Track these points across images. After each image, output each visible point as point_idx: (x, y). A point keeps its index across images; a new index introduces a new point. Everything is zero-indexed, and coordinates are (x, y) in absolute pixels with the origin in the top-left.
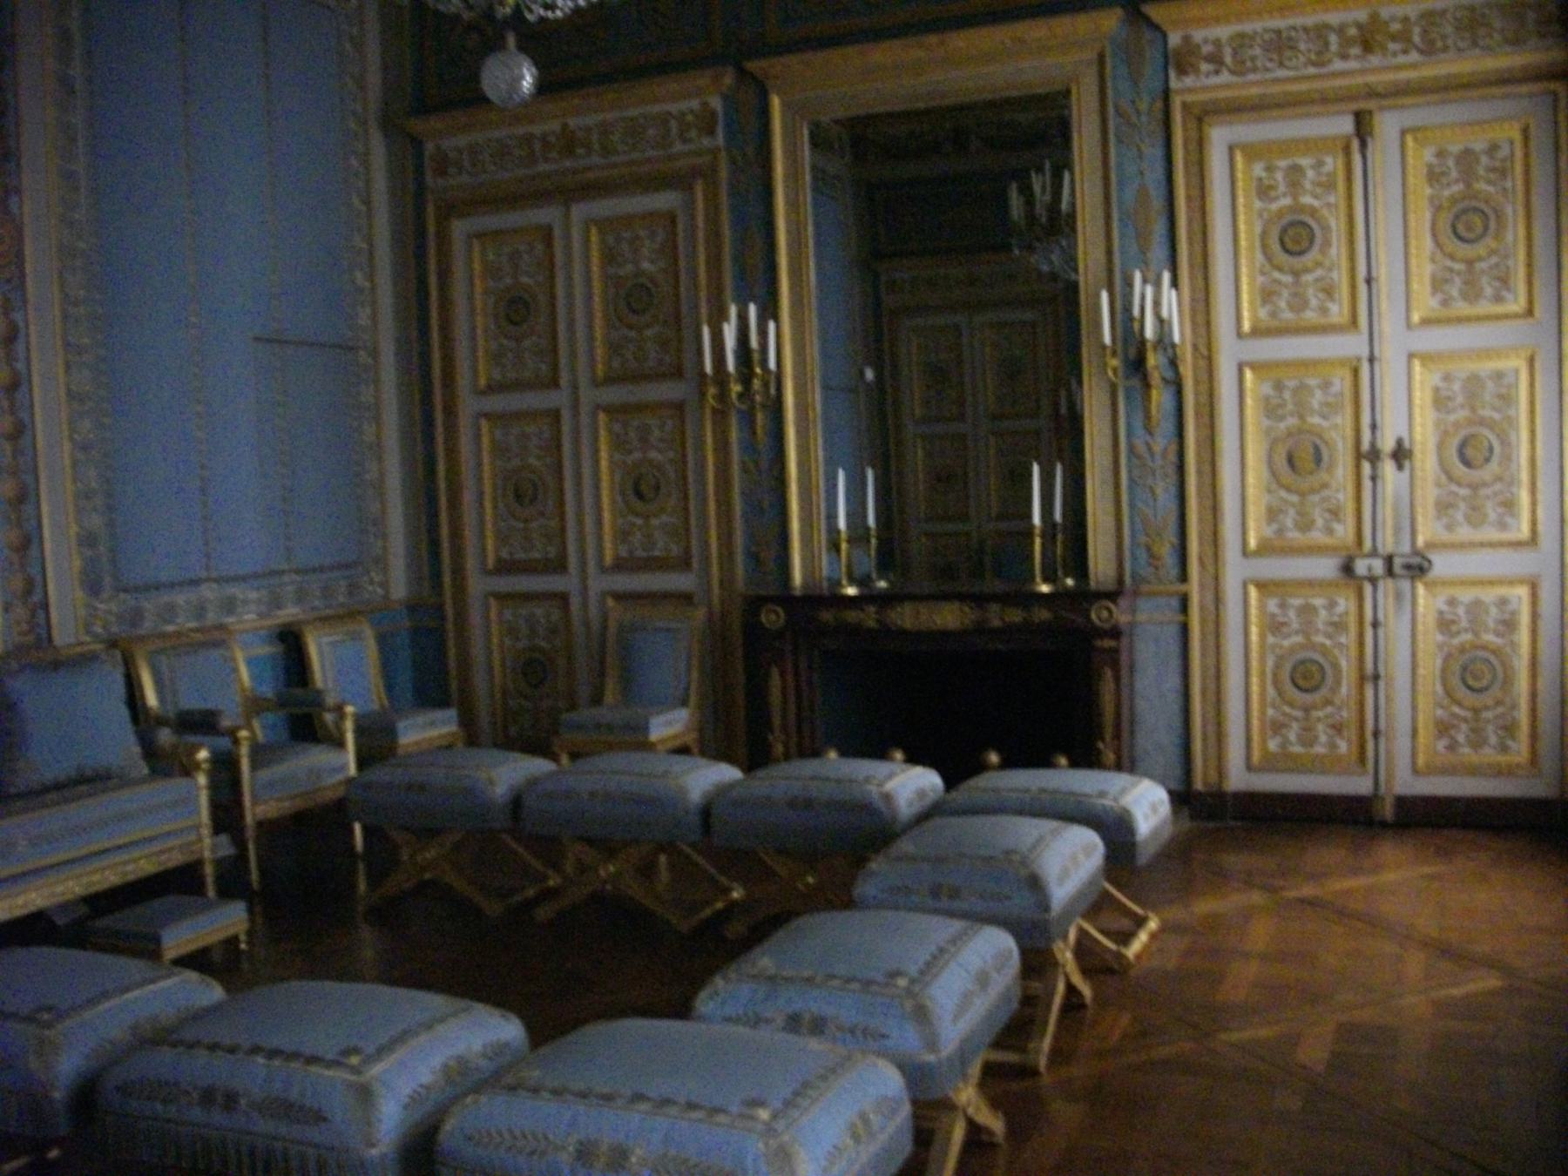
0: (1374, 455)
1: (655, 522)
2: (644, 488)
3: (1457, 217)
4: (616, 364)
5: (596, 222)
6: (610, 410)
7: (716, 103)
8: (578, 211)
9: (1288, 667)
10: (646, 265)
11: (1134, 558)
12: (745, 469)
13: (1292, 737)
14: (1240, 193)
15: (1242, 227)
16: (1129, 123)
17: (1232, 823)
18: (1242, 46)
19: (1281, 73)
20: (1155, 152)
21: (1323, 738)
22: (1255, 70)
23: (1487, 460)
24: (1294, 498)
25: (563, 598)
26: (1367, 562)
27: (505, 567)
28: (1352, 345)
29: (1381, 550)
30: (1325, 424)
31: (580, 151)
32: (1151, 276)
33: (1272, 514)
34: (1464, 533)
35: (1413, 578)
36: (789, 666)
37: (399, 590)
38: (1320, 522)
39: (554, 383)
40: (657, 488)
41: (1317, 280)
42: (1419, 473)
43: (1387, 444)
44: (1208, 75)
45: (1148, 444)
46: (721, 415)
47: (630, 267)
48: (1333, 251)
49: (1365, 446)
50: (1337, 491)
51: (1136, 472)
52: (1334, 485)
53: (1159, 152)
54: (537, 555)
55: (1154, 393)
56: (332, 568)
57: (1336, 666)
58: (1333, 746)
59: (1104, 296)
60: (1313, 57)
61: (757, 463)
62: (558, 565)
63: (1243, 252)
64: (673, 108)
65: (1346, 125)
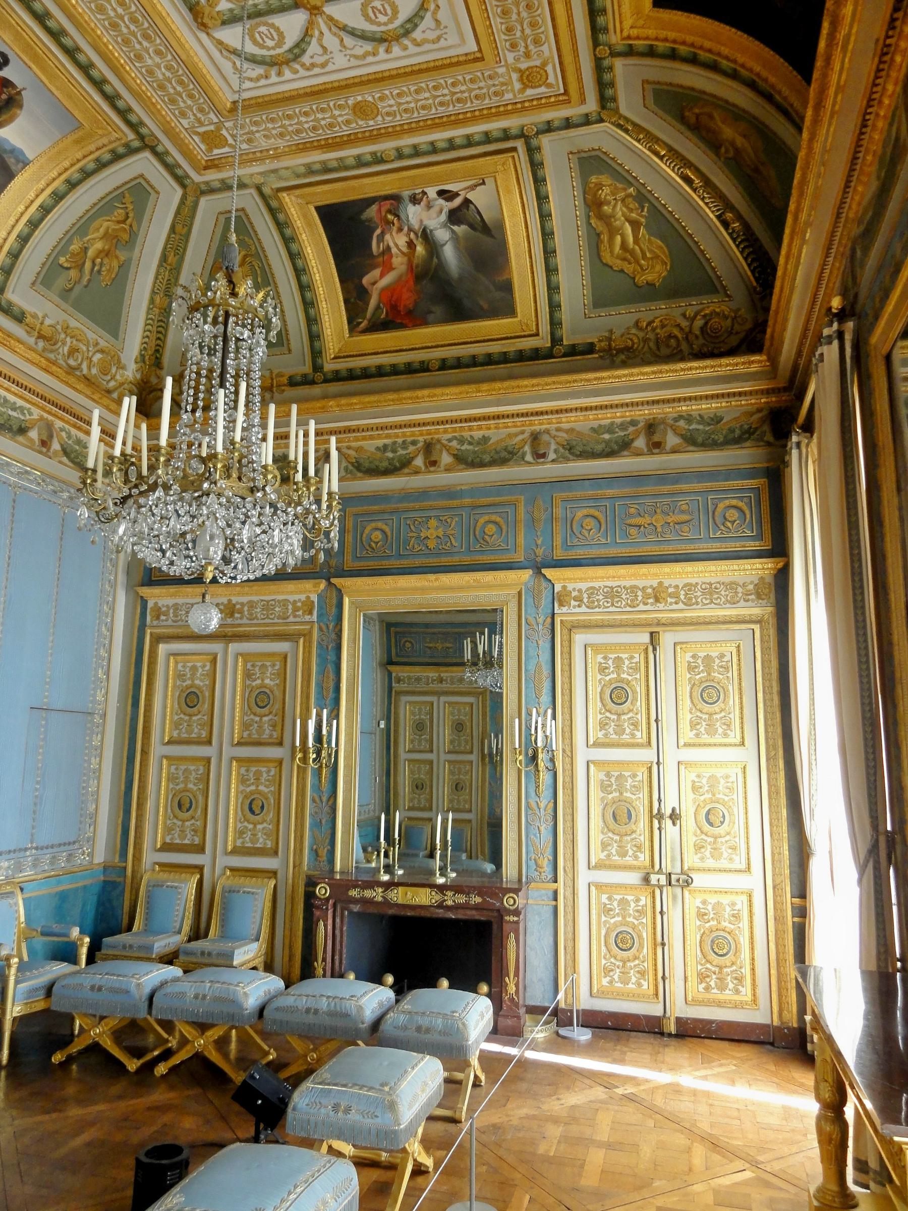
1: (260, 827)
2: (254, 807)
4: (245, 734)
5: (241, 654)
6: (239, 760)
7: (314, 598)
8: (233, 647)
10: (267, 681)
12: (313, 800)
13: (616, 977)
14: (589, 670)
15: (590, 688)
18: (592, 593)
19: (611, 609)
20: (545, 645)
21: (634, 980)
23: (722, 823)
24: (617, 838)
25: (200, 869)
27: (167, 847)
28: (649, 755)
29: (664, 871)
30: (634, 797)
31: (237, 615)
32: (541, 711)
33: (604, 846)
34: (710, 863)
36: (330, 922)
37: (100, 858)
38: (630, 853)
39: (209, 742)
40: (262, 807)
41: (629, 719)
43: (668, 812)
44: (574, 607)
46: (302, 771)
47: (259, 682)
49: (655, 811)
52: (638, 832)
53: (548, 645)
54: (186, 842)
56: (60, 845)
57: (640, 937)
59: (517, 720)
61: (320, 797)
62: (200, 849)
64: (292, 598)
65: (646, 638)
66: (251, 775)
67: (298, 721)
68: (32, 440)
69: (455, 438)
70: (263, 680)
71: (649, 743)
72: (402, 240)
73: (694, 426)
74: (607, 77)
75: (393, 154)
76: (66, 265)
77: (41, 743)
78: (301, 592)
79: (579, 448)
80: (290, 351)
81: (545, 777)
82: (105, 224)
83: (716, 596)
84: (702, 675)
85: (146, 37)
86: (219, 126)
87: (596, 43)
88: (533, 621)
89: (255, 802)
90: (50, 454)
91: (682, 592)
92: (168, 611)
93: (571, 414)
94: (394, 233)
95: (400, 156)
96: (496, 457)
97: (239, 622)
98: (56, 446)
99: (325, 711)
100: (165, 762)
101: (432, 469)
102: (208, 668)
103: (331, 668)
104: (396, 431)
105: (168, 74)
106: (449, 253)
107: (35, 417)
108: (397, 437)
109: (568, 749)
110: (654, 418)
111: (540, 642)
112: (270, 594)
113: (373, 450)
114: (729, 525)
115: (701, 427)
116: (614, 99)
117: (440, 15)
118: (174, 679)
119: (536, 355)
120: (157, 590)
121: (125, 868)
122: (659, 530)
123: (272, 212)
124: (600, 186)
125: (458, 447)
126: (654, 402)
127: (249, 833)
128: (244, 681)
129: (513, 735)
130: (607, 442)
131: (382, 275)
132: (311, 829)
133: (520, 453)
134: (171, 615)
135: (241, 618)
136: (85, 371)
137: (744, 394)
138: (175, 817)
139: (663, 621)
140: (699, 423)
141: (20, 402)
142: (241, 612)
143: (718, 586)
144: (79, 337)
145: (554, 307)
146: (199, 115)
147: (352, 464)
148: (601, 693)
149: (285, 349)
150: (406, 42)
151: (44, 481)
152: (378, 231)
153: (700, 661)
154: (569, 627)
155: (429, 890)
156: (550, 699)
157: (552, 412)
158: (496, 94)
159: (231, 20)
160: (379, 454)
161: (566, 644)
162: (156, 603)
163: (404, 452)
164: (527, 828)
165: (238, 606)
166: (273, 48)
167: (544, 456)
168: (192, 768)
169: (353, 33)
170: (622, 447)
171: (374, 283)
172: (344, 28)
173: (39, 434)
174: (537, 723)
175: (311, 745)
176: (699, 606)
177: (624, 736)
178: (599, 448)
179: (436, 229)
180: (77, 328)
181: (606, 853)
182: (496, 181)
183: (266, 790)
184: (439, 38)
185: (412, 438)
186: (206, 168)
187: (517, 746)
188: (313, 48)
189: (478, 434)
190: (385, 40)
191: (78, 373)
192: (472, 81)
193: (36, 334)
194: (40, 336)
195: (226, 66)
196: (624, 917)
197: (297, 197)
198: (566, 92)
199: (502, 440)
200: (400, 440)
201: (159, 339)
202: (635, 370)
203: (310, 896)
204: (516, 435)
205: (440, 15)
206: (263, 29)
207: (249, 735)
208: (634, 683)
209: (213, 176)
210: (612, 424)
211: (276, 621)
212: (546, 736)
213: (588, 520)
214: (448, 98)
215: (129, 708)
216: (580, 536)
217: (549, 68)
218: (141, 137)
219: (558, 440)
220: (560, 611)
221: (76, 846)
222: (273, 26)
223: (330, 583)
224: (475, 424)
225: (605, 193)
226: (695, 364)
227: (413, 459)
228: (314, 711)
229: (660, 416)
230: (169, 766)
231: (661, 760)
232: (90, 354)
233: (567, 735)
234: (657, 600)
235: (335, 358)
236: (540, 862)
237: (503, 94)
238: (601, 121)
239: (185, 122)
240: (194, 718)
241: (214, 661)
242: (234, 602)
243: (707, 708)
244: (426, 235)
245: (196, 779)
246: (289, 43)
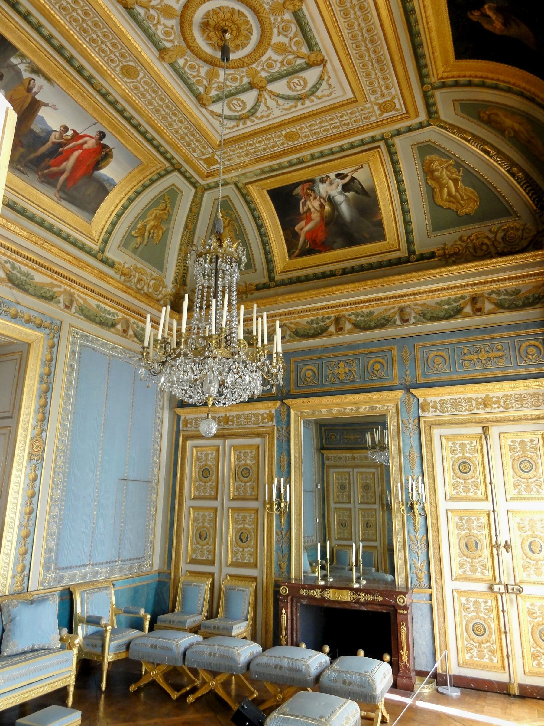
1: (246, 550)
2: (242, 537)
3: (521, 463)
5: (233, 446)
6: (233, 509)
7: (274, 411)
8: (229, 442)
10: (248, 462)
11: (411, 578)
12: (277, 534)
13: (475, 654)
14: (444, 451)
18: (443, 403)
20: (415, 436)
21: (487, 656)
22: (448, 411)
23: (541, 551)
25: (212, 575)
26: (499, 586)
28: (488, 505)
29: (503, 583)
30: (479, 533)
31: (230, 423)
32: (415, 478)
33: (461, 565)
34: (534, 578)
36: (289, 610)
37: (156, 567)
38: (479, 570)
39: (216, 498)
40: (247, 538)
41: (472, 482)
43: (503, 543)
44: (432, 412)
46: (270, 516)
47: (243, 462)
48: (478, 472)
49: (494, 543)
51: (411, 546)
53: (417, 436)
54: (204, 558)
55: (417, 518)
56: (134, 559)
57: (489, 627)
58: (491, 660)
62: (212, 563)
64: (261, 412)
65: (480, 431)
66: (240, 518)
67: (267, 485)
68: (119, 330)
69: (353, 313)
70: (246, 461)
71: (487, 498)
72: (316, 204)
73: (502, 297)
74: (431, 101)
75: (309, 157)
76: (135, 235)
77: (124, 499)
78: (266, 409)
79: (429, 315)
80: (256, 270)
81: (420, 520)
82: (155, 212)
83: (525, 402)
84: (519, 453)
85: (174, 114)
86: (213, 154)
87: (423, 84)
88: (406, 422)
89: (243, 535)
90: (128, 337)
91: (502, 401)
92: (192, 421)
93: (423, 295)
94: (312, 200)
95: (313, 157)
96: (378, 323)
97: (231, 427)
98: (131, 332)
99: (282, 479)
100: (191, 510)
101: (340, 332)
102: (214, 455)
103: (285, 453)
104: (318, 312)
105: (186, 131)
106: (345, 209)
107: (120, 317)
108: (319, 315)
109: (433, 502)
110: (476, 294)
111: (412, 435)
112: (248, 410)
113: (305, 323)
114: (530, 357)
115: (506, 297)
116: (436, 112)
117: (331, 82)
118: (196, 461)
119: (399, 262)
120: (185, 410)
121: (170, 574)
122: (484, 362)
123: (244, 196)
124: (432, 161)
125: (355, 319)
126: (475, 284)
127: (240, 553)
128: (235, 462)
129: (397, 493)
130: (447, 311)
131: (306, 224)
132: (276, 552)
133: (392, 320)
134: (194, 424)
135: (232, 425)
136: (146, 291)
137: (534, 275)
138: (198, 543)
139: (490, 419)
140: (505, 295)
141: (112, 310)
142: (232, 421)
143: (526, 396)
144: (143, 273)
145: (408, 233)
146: (202, 150)
147: (293, 332)
148: (452, 466)
149: (253, 270)
150: (313, 98)
151: (125, 352)
152: (303, 200)
153: (517, 444)
154: (429, 425)
155: (349, 592)
156: (420, 470)
157: (411, 295)
158: (366, 118)
159: (218, 99)
160: (309, 326)
161: (428, 435)
162: (185, 418)
163: (324, 324)
164: (409, 553)
165: (230, 418)
166: (241, 111)
167: (407, 321)
168: (207, 514)
169: (283, 97)
170: (457, 312)
171: (302, 229)
172: (278, 96)
173: (122, 327)
174: (412, 485)
175: (274, 500)
176: (514, 409)
177: (470, 494)
178: (442, 314)
179: (336, 196)
180: (141, 268)
181: (462, 570)
182: (369, 166)
183: (249, 527)
184: (331, 94)
185: (328, 315)
186: (207, 177)
188: (262, 107)
189: (366, 311)
190: (301, 99)
191: (142, 292)
192: (351, 113)
193: (120, 273)
194: (123, 274)
195: (216, 123)
196: (477, 613)
197: (257, 186)
198: (407, 112)
199: (381, 313)
200: (320, 317)
201: (184, 270)
202: (461, 266)
203: (277, 593)
204: (390, 309)
205: (331, 82)
206: (235, 102)
207: (239, 494)
208: (474, 459)
209: (211, 181)
210: (449, 299)
211: (252, 426)
212: (419, 494)
213: (437, 358)
214: (338, 124)
215: (172, 478)
216: (433, 368)
217: (396, 101)
218: (173, 165)
219: (416, 310)
220: (423, 415)
221: (143, 560)
222: (240, 100)
223: (283, 403)
224: (364, 304)
225: (435, 165)
226: (499, 260)
227: (328, 327)
228: (276, 479)
229: (479, 292)
230: (194, 513)
231: (495, 509)
232: (148, 281)
233: (432, 493)
234: (486, 406)
235: (281, 272)
236: (419, 575)
237: (370, 118)
238: (430, 125)
239: (195, 155)
240: (208, 484)
241: (218, 450)
242: (228, 415)
243: (524, 475)
244: (330, 200)
245: (209, 520)
246: (249, 107)
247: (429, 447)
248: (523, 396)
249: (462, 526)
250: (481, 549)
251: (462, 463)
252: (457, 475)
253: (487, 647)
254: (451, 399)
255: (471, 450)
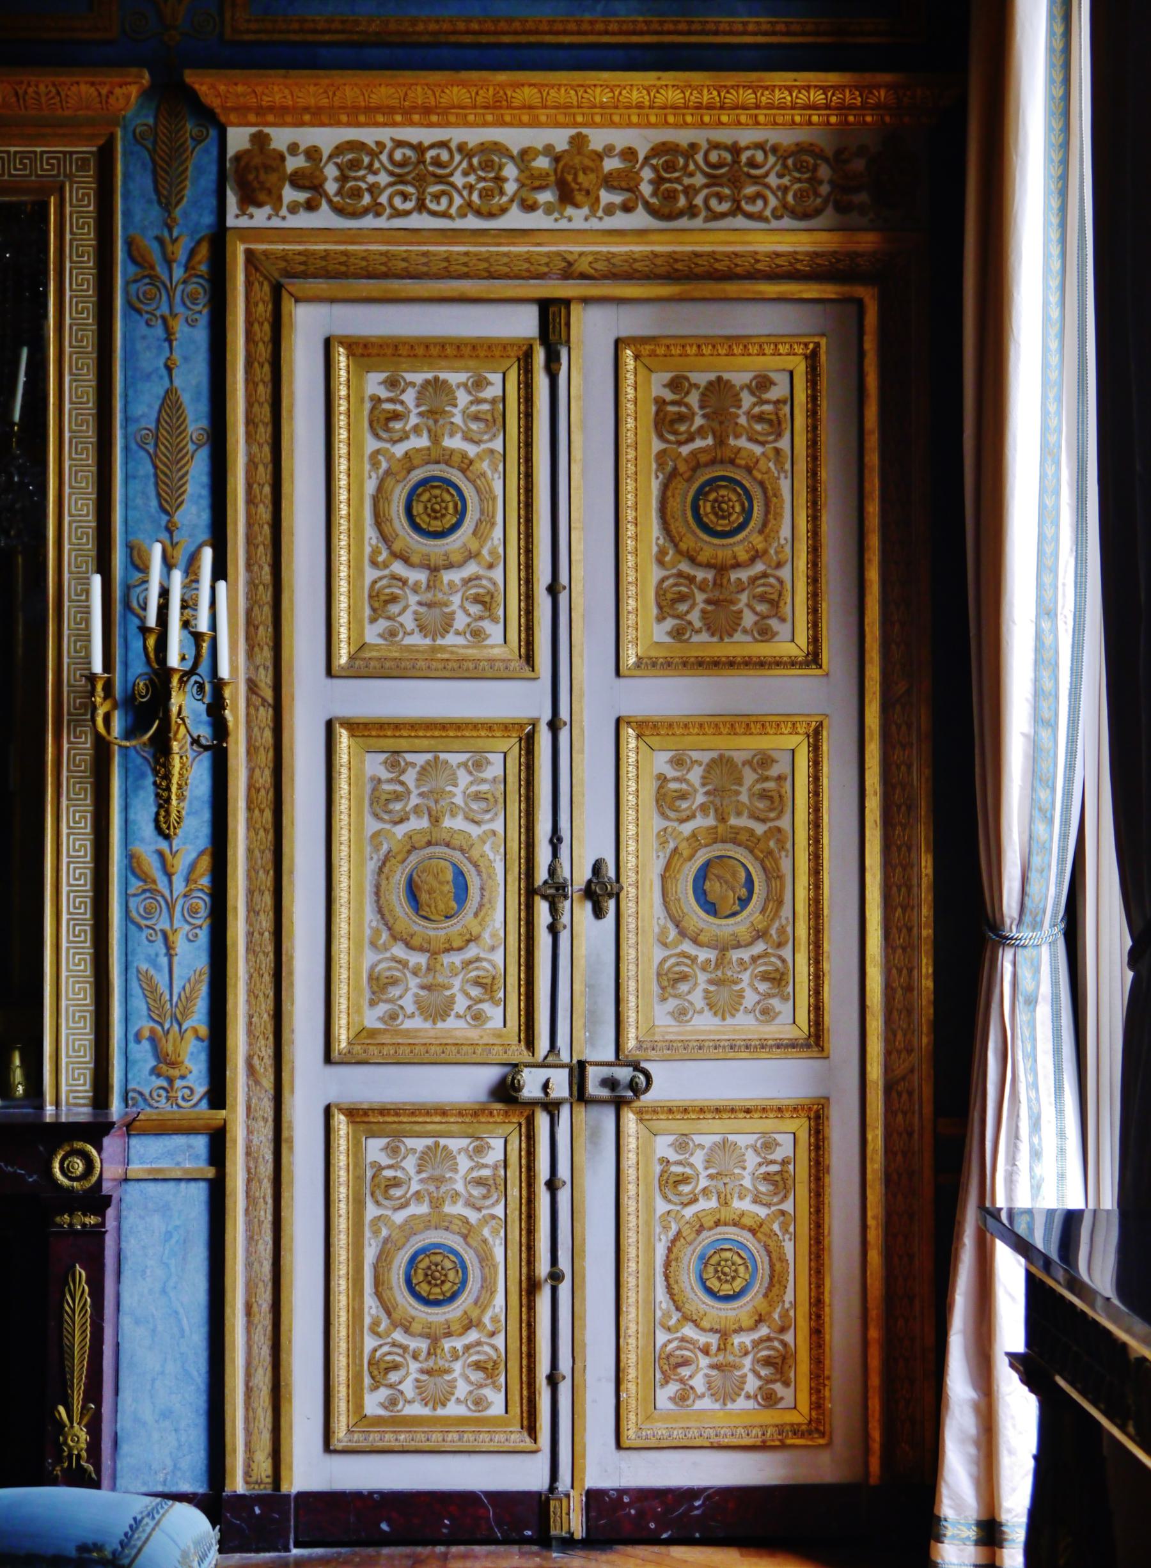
0: (556, 892)
3: (701, 493)
9: (401, 1260)
13: (408, 1387)
14: (341, 421)
16: (153, 279)
17: (295, 1551)
18: (355, 165)
19: (418, 221)
21: (462, 1389)
22: (376, 209)
24: (419, 959)
26: (543, 1074)
29: (565, 1057)
30: (475, 831)
32: (181, 556)
33: (379, 985)
35: (619, 1104)
38: (461, 1004)
41: (467, 582)
42: (629, 922)
43: (583, 874)
44: (293, 209)
45: (161, 854)
49: (542, 875)
50: (493, 949)
53: (201, 335)
55: (176, 762)
57: (485, 1259)
58: (479, 1402)
59: (97, 581)
60: (475, 197)
63: (342, 525)
71: (529, 659)
83: (750, 190)
84: (699, 443)
91: (647, 174)
109: (265, 679)
139: (583, 266)
143: (759, 156)
148: (376, 500)
153: (693, 399)
164: (126, 938)
174: (165, 593)
176: (698, 222)
177: (450, 640)
181: (382, 1008)
187: (97, 667)
196: (437, 1204)
208: (485, 466)
212: (197, 637)
220: (244, 222)
231: (564, 714)
247: (264, 392)
248: (744, 157)
249: (398, 797)
250: (481, 906)
251: (424, 482)
252: (397, 546)
253: (467, 1348)
254: (399, 144)
255: (476, 418)
